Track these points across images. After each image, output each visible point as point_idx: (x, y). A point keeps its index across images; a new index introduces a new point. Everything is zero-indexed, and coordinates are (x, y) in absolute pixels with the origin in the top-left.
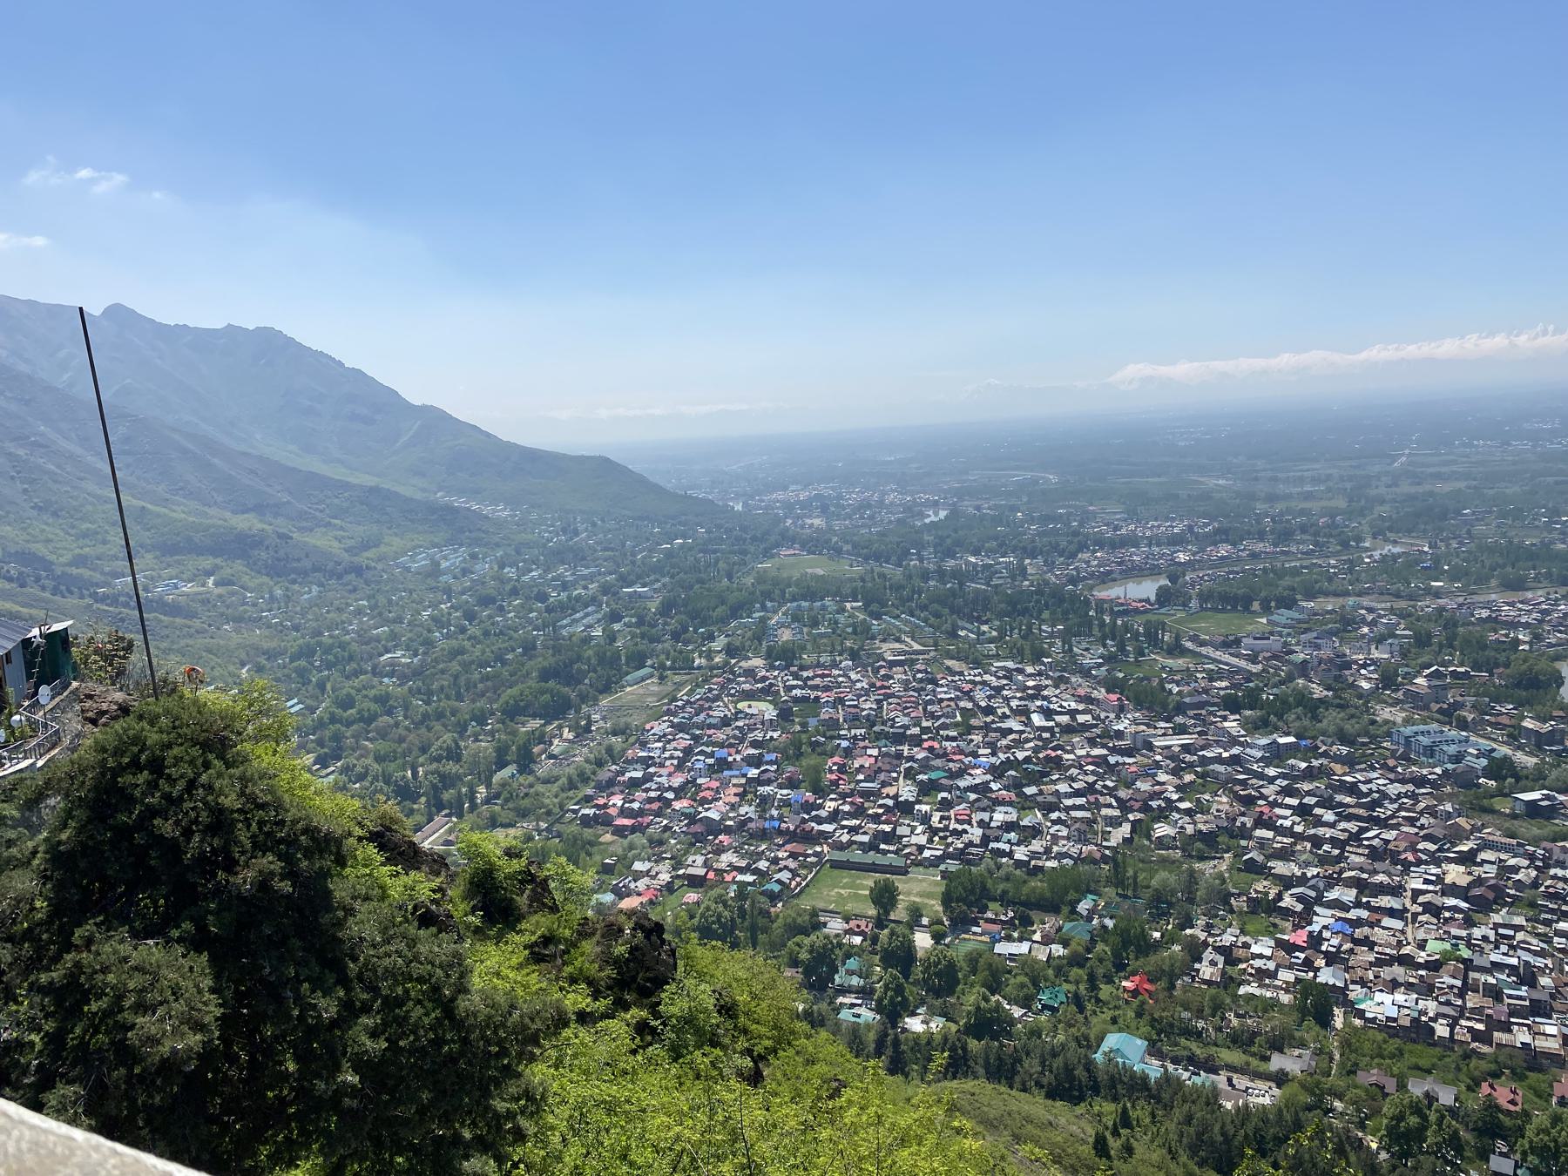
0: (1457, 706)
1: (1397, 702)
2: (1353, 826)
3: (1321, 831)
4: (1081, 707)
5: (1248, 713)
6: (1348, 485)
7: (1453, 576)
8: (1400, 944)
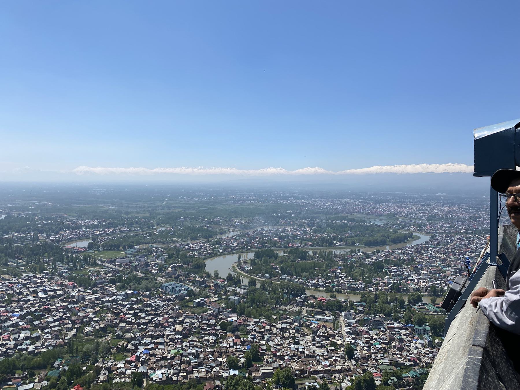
0: (180, 275)
1: (163, 276)
2: (149, 318)
4: (59, 288)
5: (118, 284)
6: (150, 209)
7: (179, 237)
8: (163, 353)
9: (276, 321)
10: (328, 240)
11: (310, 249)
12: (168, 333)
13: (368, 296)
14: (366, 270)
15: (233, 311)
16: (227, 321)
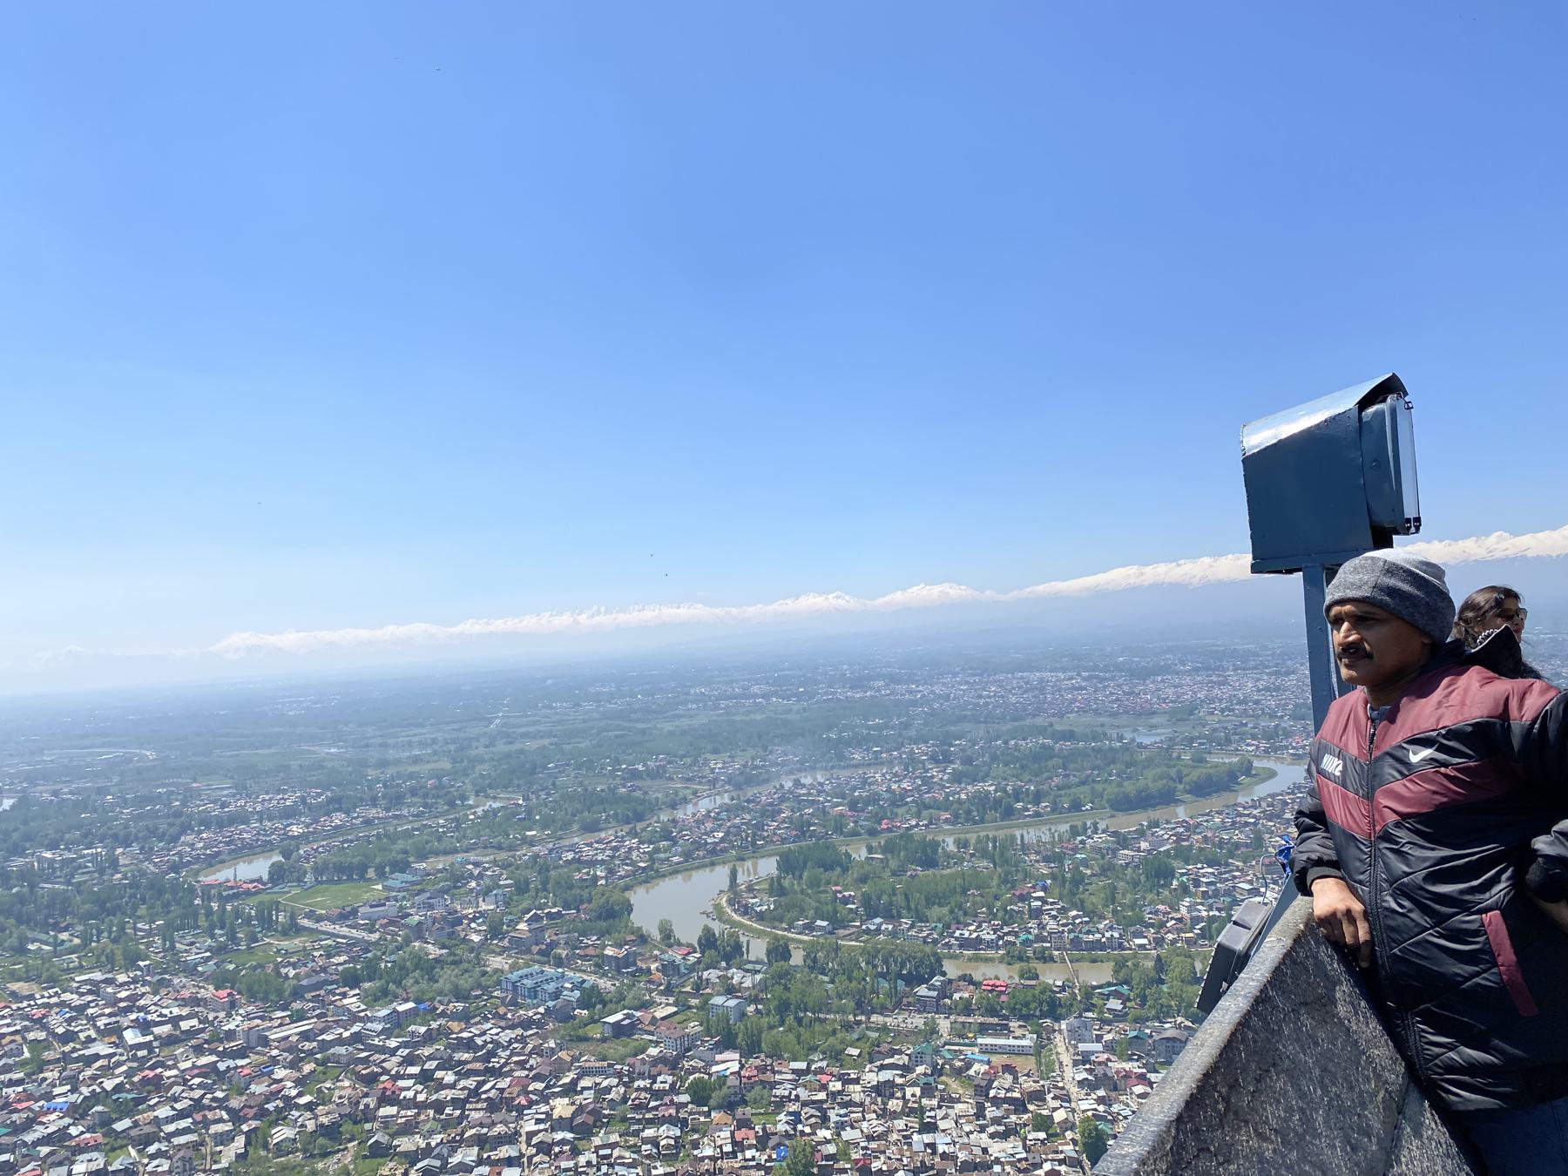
0: (553, 945)
1: (505, 949)
2: (470, 1083)
3: (447, 1094)
4: (186, 1011)
5: (367, 985)
6: (452, 747)
7: (544, 828)
9: (858, 1063)
10: (998, 802)
11: (951, 833)
12: (530, 1126)
13: (1136, 965)
14: (1121, 885)
15: (727, 1043)
16: (710, 1075)
